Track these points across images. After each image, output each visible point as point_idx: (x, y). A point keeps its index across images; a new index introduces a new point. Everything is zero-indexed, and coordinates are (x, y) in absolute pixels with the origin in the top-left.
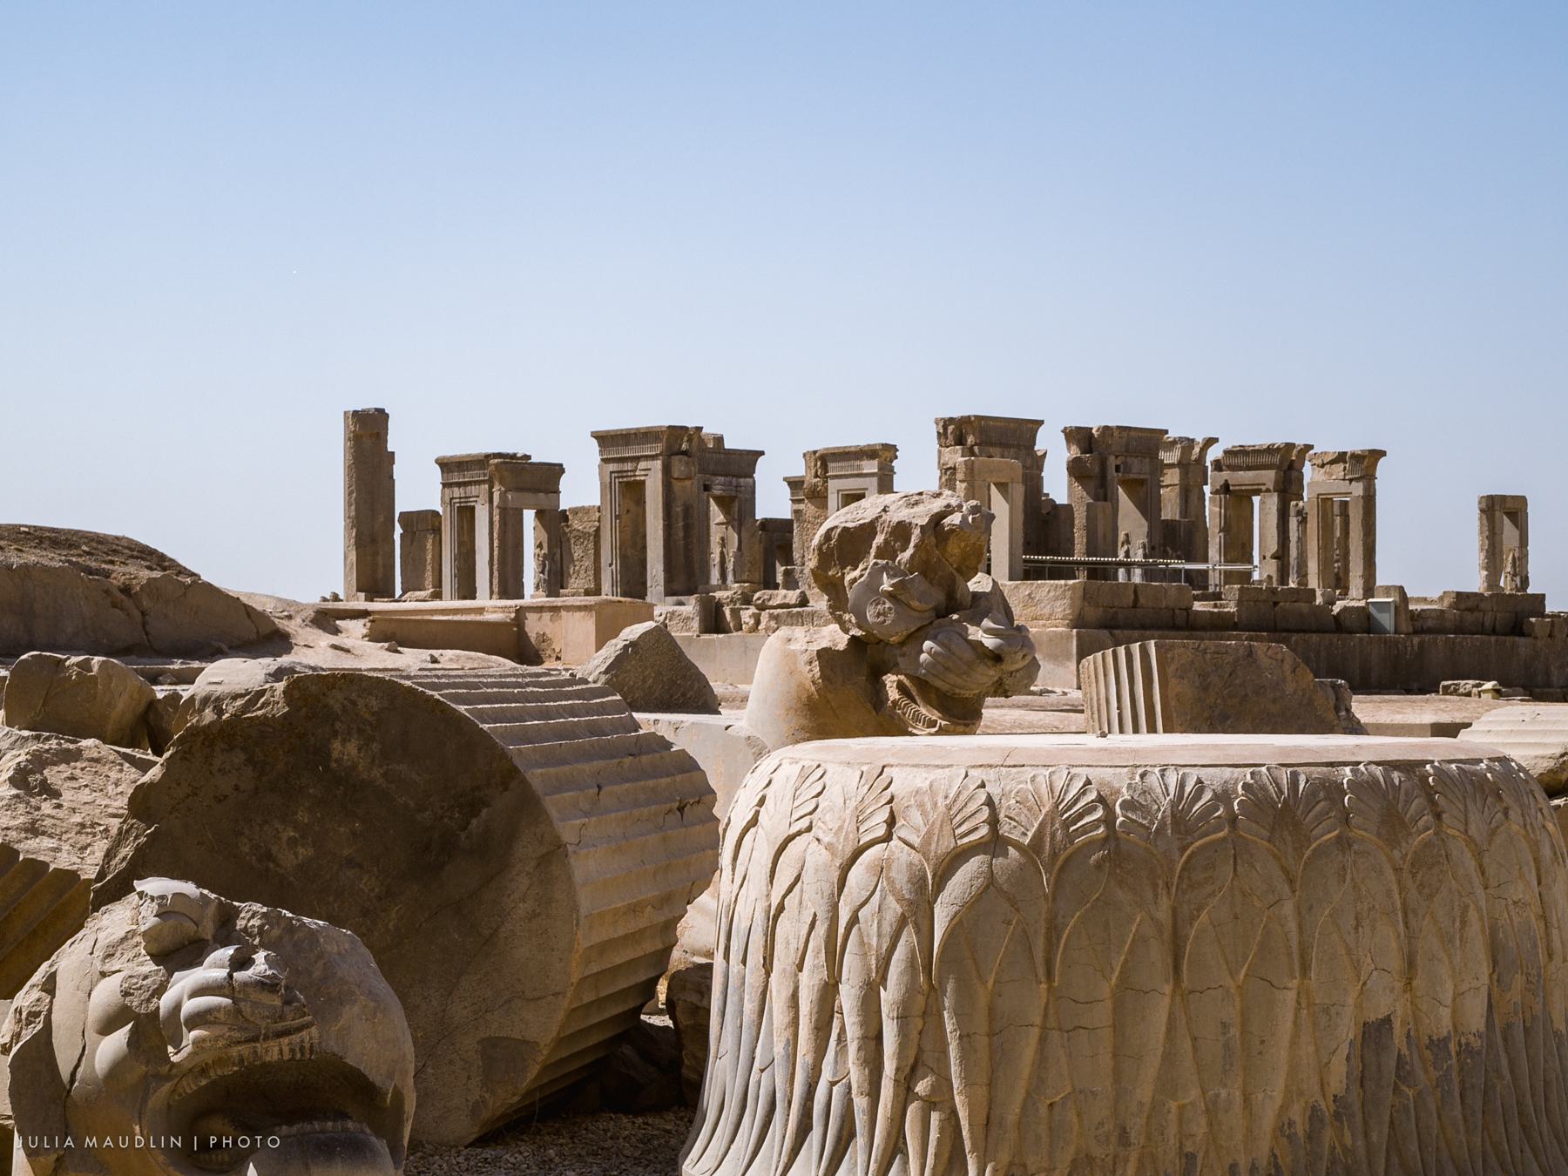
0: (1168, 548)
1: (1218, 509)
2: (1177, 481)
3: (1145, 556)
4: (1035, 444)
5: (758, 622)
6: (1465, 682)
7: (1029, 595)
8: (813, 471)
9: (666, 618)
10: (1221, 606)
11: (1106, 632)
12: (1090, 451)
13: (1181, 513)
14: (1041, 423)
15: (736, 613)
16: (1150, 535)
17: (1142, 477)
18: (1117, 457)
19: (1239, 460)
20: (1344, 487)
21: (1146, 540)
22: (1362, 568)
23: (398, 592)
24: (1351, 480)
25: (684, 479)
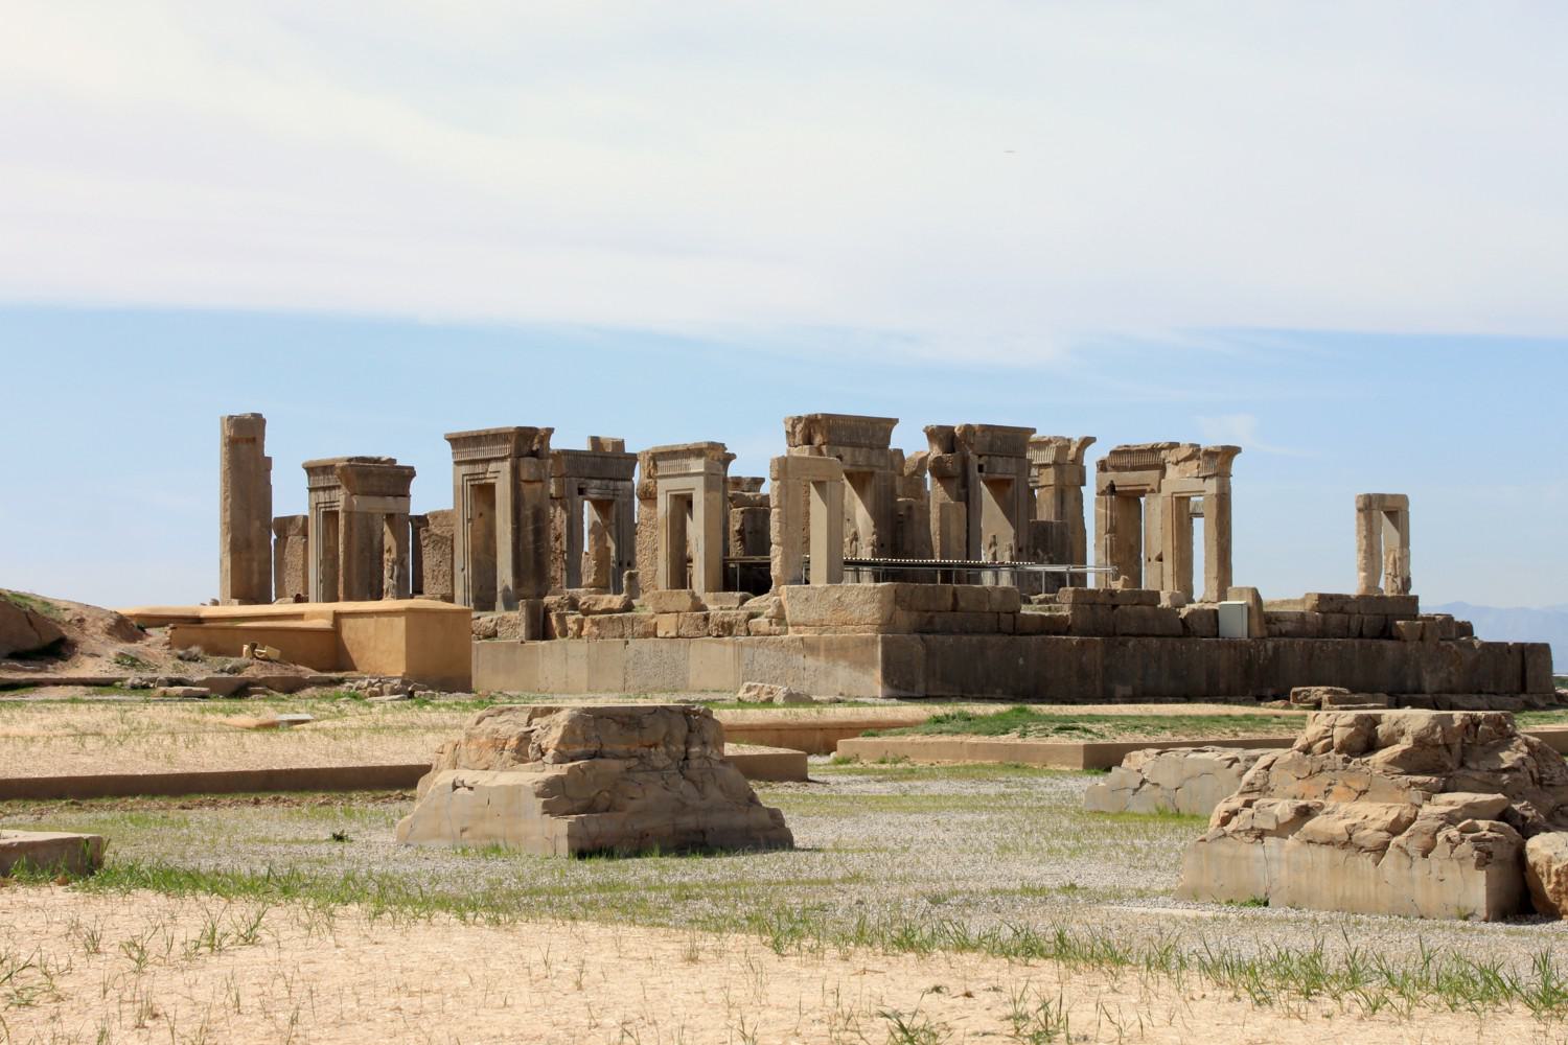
0: (1039, 551)
1: (1104, 511)
2: (1052, 482)
3: (1012, 559)
4: (888, 442)
5: (581, 628)
6: (1315, 688)
7: (839, 599)
8: (647, 471)
9: (496, 624)
10: (1057, 610)
11: (917, 636)
12: (952, 451)
13: (1056, 513)
14: (894, 422)
15: (561, 618)
16: (1017, 537)
17: (1008, 477)
18: (980, 456)
19: (1124, 460)
20: (1198, 484)
21: (1012, 542)
22: (1216, 569)
23: (274, 598)
24: (1205, 478)
25: (534, 482)
